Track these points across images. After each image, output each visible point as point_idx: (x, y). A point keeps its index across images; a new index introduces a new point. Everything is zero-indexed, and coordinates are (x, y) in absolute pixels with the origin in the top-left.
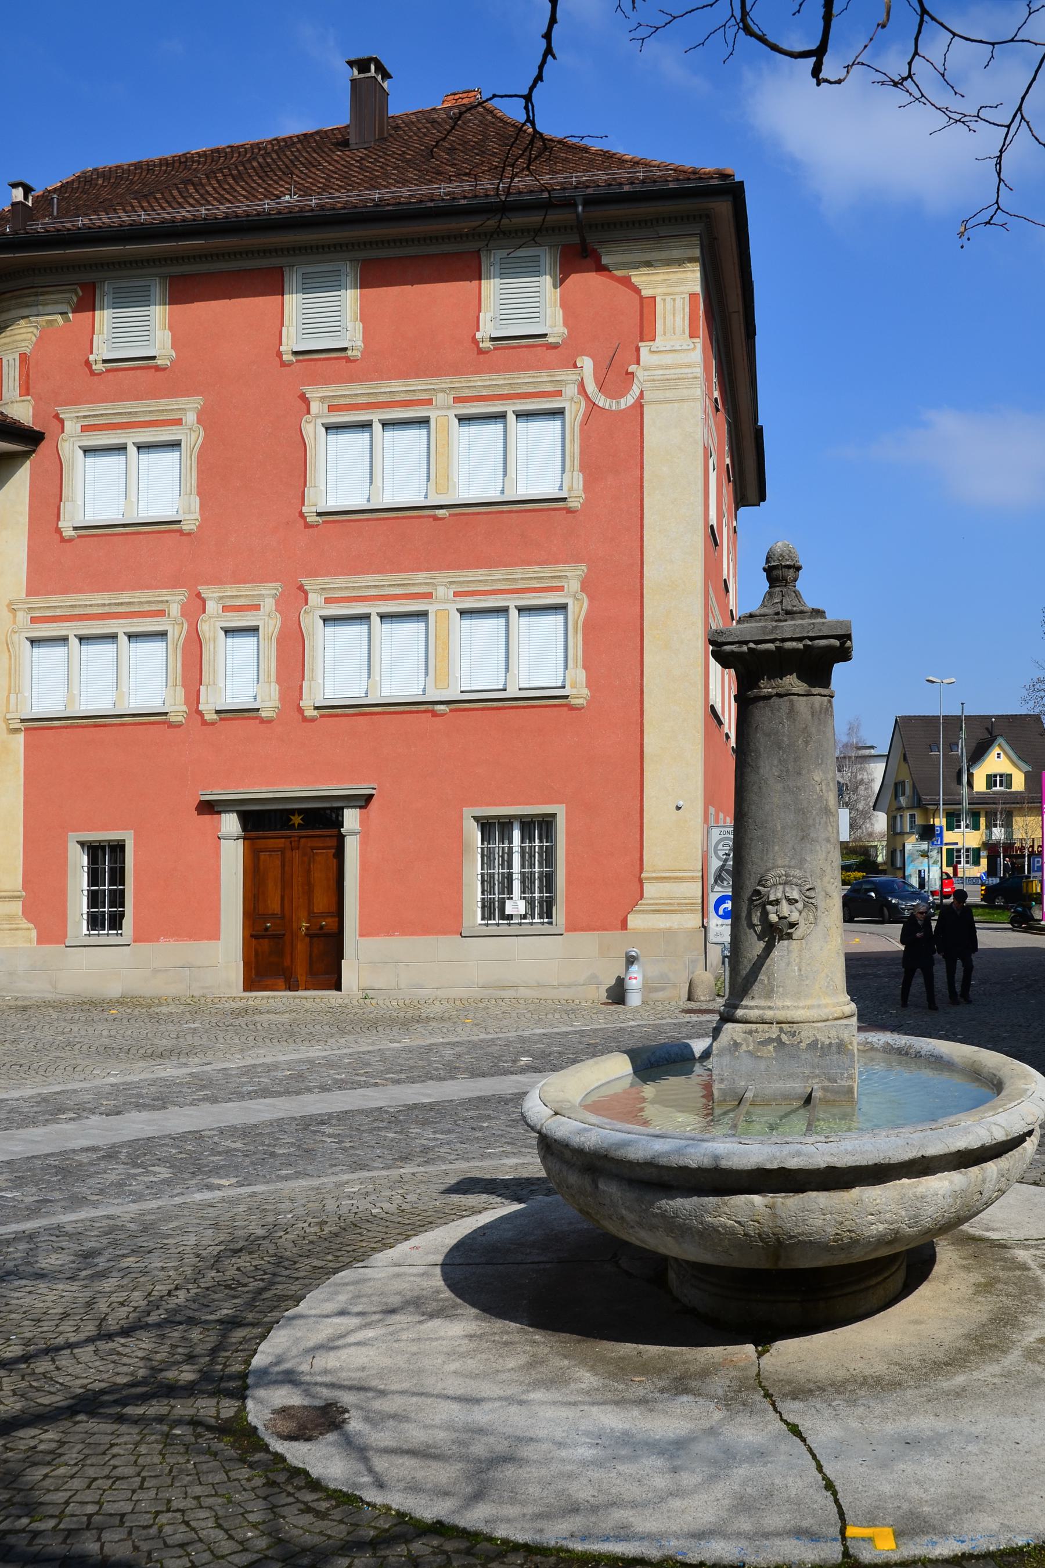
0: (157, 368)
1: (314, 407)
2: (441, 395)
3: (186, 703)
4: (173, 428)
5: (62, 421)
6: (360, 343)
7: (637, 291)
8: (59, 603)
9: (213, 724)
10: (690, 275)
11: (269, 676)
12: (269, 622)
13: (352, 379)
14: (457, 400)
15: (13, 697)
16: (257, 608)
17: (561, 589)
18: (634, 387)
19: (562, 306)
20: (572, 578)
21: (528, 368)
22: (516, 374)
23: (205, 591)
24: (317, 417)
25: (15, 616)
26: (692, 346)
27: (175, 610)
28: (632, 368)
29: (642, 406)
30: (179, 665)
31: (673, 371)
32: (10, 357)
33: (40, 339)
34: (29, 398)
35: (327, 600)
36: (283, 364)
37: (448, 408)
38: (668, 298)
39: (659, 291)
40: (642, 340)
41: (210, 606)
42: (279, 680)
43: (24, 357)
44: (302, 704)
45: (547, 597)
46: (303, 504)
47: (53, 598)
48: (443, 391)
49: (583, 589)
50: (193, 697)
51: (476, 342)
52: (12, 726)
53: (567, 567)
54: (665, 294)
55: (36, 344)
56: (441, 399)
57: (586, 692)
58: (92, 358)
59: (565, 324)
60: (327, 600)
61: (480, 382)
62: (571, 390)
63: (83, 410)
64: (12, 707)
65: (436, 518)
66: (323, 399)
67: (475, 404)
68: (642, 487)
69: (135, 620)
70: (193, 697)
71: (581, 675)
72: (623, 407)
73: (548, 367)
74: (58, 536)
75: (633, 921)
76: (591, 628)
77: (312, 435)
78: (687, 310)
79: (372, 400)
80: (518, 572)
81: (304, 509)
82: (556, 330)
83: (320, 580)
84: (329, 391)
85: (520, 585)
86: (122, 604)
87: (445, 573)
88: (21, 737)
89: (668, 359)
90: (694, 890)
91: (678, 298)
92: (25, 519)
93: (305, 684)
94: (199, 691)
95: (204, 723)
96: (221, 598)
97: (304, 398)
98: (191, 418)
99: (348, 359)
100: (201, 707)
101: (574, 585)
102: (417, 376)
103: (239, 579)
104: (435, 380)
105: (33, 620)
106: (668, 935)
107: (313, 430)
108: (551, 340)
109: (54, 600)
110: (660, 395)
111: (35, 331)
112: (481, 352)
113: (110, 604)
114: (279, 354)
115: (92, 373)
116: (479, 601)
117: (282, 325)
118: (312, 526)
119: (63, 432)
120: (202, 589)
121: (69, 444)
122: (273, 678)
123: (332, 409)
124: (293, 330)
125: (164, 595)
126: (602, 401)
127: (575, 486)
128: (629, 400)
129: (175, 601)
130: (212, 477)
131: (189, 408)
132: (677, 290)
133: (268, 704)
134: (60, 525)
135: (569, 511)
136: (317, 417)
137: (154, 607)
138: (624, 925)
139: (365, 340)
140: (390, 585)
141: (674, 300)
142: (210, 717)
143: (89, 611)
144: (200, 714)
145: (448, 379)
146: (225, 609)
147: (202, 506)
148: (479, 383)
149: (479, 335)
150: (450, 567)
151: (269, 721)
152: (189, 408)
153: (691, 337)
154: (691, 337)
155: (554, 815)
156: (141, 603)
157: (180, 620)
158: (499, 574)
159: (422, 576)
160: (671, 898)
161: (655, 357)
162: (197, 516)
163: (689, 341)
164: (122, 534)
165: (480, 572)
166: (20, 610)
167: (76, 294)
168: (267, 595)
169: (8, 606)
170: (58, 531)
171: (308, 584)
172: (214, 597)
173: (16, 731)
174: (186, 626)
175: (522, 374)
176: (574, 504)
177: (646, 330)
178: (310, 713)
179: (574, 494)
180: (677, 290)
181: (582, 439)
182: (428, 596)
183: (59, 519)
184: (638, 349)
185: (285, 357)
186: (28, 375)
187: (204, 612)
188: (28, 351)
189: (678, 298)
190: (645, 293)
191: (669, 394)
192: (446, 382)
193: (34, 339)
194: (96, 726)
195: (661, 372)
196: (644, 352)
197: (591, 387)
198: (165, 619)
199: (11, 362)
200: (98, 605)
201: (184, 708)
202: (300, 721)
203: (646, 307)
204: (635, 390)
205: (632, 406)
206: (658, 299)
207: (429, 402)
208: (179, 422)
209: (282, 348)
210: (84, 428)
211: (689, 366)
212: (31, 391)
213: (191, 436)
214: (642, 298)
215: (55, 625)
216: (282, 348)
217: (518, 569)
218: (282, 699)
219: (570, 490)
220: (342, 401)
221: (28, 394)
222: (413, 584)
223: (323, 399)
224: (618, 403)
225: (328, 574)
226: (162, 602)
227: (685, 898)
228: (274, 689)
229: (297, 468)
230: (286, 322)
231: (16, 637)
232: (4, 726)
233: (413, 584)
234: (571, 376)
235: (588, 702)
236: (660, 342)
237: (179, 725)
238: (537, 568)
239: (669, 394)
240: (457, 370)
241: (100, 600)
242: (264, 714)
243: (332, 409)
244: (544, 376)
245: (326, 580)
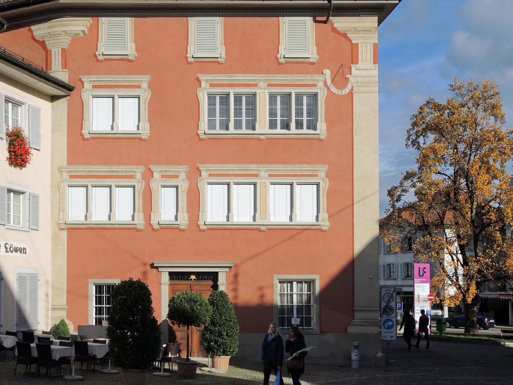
0: (129, 60)
1: (203, 84)
2: (261, 83)
3: (145, 220)
4: (137, 89)
5: (83, 83)
6: (224, 56)
7: (350, 41)
9: (157, 230)
10: (373, 35)
11: (183, 209)
13: (220, 72)
14: (269, 85)
15: (61, 213)
16: (177, 177)
17: (316, 176)
18: (349, 85)
19: (317, 45)
20: (322, 170)
21: (301, 72)
22: (296, 75)
23: (153, 168)
24: (204, 89)
25: (62, 175)
26: (375, 68)
27: (139, 176)
28: (348, 76)
29: (352, 94)
30: (141, 202)
31: (366, 79)
32: (56, 50)
33: (72, 42)
34: (66, 70)
35: (210, 175)
36: (188, 63)
37: (265, 89)
38: (364, 45)
39: (360, 41)
40: (352, 63)
41: (155, 174)
42: (188, 212)
43: (64, 51)
44: (199, 223)
45: (310, 179)
46: (198, 129)
47: (81, 166)
48: (263, 81)
49: (327, 176)
50: (148, 218)
51: (277, 59)
52: (61, 227)
53: (319, 166)
54: (363, 43)
55: (70, 44)
56: (261, 84)
57: (328, 223)
58: (97, 53)
59: (318, 54)
60: (210, 175)
61: (279, 78)
62: (321, 84)
63: (93, 78)
64: (61, 218)
65: (259, 140)
66: (207, 81)
67: (277, 88)
68: (352, 131)
69: (120, 179)
70: (148, 218)
72: (344, 93)
73: (309, 73)
74: (81, 137)
75: (351, 330)
76: (330, 194)
77: (202, 97)
78: (372, 51)
79: (230, 83)
80: (297, 167)
81: (199, 132)
82: (314, 56)
83: (206, 165)
84: (210, 77)
85: (298, 173)
86: (113, 171)
87: (264, 165)
88: (65, 233)
89: (364, 73)
91: (368, 45)
92: (65, 128)
93: (200, 214)
94: (150, 215)
95: (153, 230)
96: (161, 171)
98: (145, 85)
99: (218, 63)
100: (152, 222)
101: (323, 174)
102: (251, 73)
103: (169, 163)
104: (258, 75)
105: (71, 177)
108: (311, 60)
109: (81, 168)
111: (69, 38)
112: (280, 64)
113: (107, 171)
114: (186, 58)
115: (98, 60)
116: (280, 179)
117: (188, 44)
118: (202, 140)
119: (83, 87)
120: (151, 166)
121: (86, 93)
122: (185, 210)
123: (211, 85)
124: (192, 47)
125: (133, 168)
126: (333, 89)
127: (323, 129)
128: (346, 91)
131: (144, 80)
132: (368, 41)
133: (183, 222)
134: (83, 132)
135: (320, 140)
136: (204, 89)
137: (129, 174)
139: (226, 54)
140: (239, 170)
141: (367, 46)
142: (156, 227)
143: (98, 174)
144: (151, 225)
145: (264, 75)
146: (163, 176)
147: (150, 127)
148: (279, 78)
149: (279, 56)
150: (266, 163)
151: (184, 231)
152: (144, 80)
153: (374, 63)
154: (374, 63)
156: (122, 171)
157: (141, 181)
158: (289, 167)
159: (253, 166)
160: (367, 319)
161: (358, 72)
162: (148, 132)
163: (373, 65)
164: (113, 138)
165: (281, 166)
166: (64, 171)
167: (89, 22)
168: (182, 171)
169: (59, 169)
170: (82, 135)
171: (201, 167)
172: (157, 170)
173: (63, 229)
174: (144, 183)
175: (298, 75)
176: (323, 137)
177: (354, 59)
178: (203, 227)
179: (323, 132)
180: (368, 41)
181: (326, 107)
182: (257, 175)
183: (82, 129)
184: (350, 68)
185: (189, 60)
186: (66, 59)
187: (153, 177)
188: (66, 48)
189: (368, 45)
190: (354, 42)
191: (364, 89)
192: (263, 77)
193: (69, 42)
194: (102, 229)
195: (361, 79)
196: (353, 69)
197: (329, 82)
198: (134, 180)
199: (57, 52)
200: (102, 171)
201: (144, 222)
202: (197, 232)
203: (354, 48)
204: (349, 86)
205: (348, 94)
206: (359, 45)
207: (256, 85)
208: (139, 87)
209: (188, 55)
210: (94, 87)
211: (373, 77)
212: (67, 67)
213: (146, 94)
214: (352, 44)
215: (81, 179)
216: (188, 55)
217: (297, 166)
218: (190, 220)
219: (321, 130)
220: (216, 82)
221: (66, 68)
222: (250, 170)
223: (207, 81)
224: (342, 92)
225: (210, 163)
226: (132, 171)
227: (373, 320)
230: (189, 43)
231: (62, 184)
232: (57, 226)
233: (250, 170)
234: (320, 78)
235: (329, 228)
236: (360, 65)
237: (141, 231)
238: (306, 166)
239: (364, 89)
240: (268, 71)
242: (181, 227)
244: (308, 77)
245: (210, 165)
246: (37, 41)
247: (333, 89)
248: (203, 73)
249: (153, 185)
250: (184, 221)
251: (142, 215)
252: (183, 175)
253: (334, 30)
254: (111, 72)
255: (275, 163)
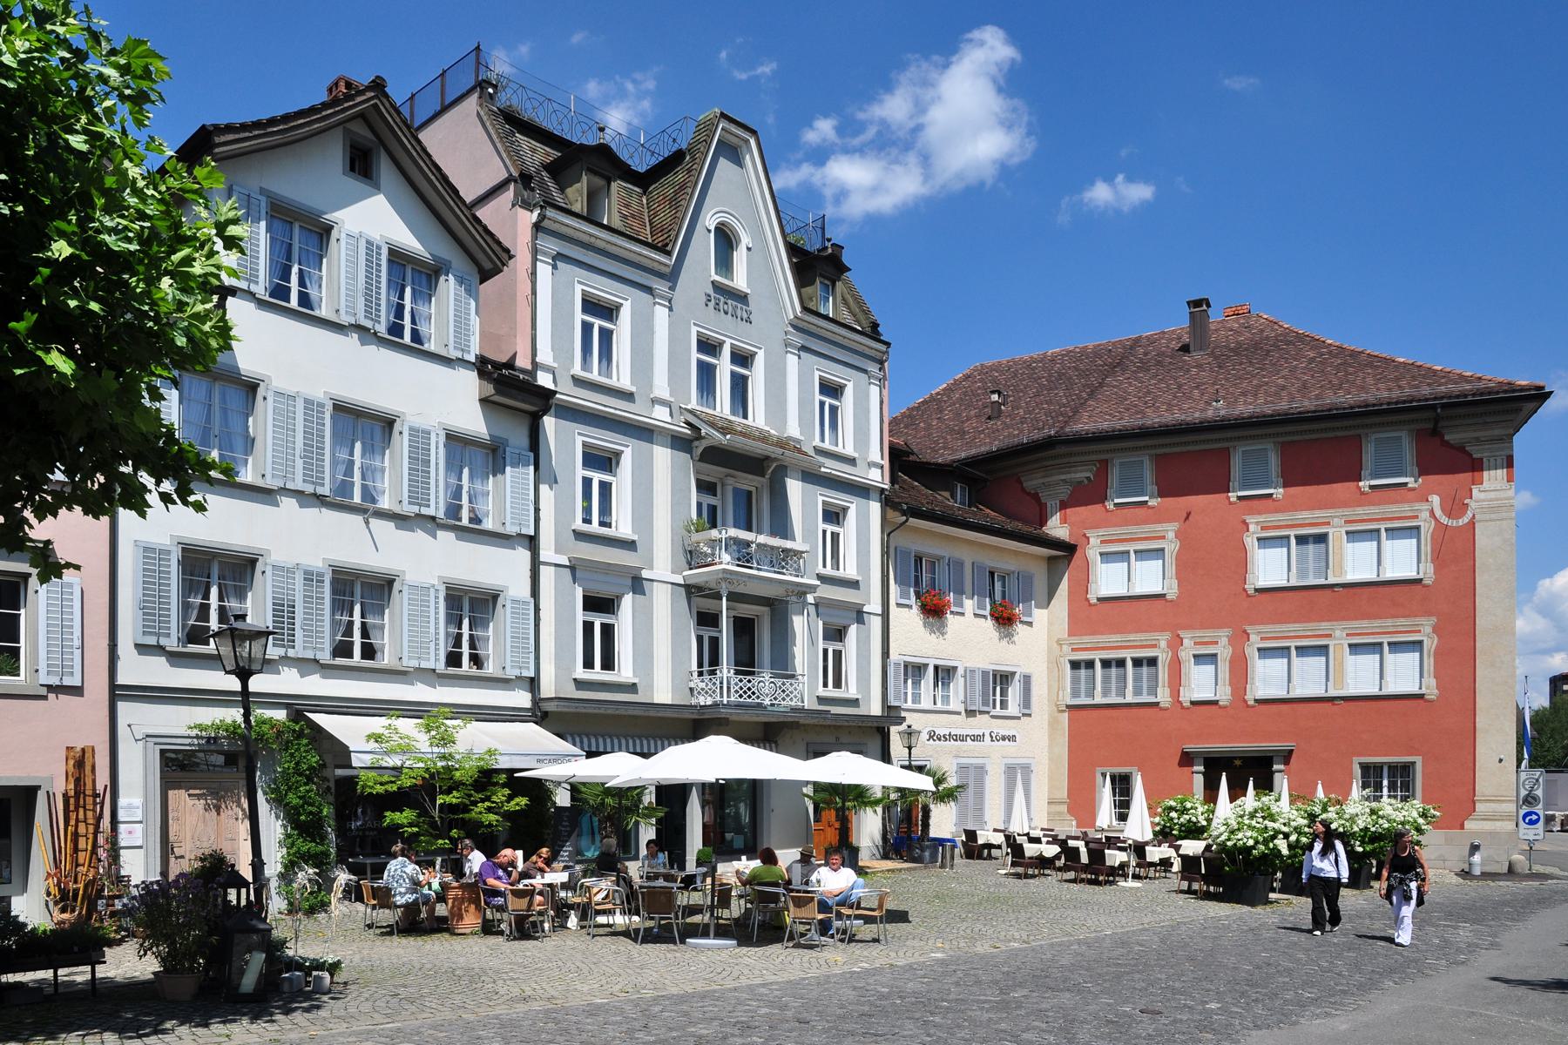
1: (1252, 528)
8: (1088, 640)
12: (1224, 651)
13: (1277, 511)
21: (1396, 502)
27: (1163, 644)
41: (1186, 642)
49: (1436, 630)
71: (1433, 682)
75: (1468, 825)
80: (1389, 622)
84: (1261, 518)
89: (1492, 495)
90: (1512, 807)
97: (1244, 522)
98: (1171, 535)
103: (1203, 626)
106: (1493, 835)
107: (1250, 541)
109: (1086, 639)
110: (1487, 517)
121: (1093, 550)
123: (1263, 528)
125: (1155, 636)
126: (1444, 520)
128: (1466, 520)
129: (1163, 640)
130: (1185, 568)
138: (1462, 827)
150: (1344, 619)
155: (1414, 763)
158: (1377, 623)
159: (1325, 625)
168: (1223, 636)
171: (1249, 629)
176: (1427, 582)
192: (1340, 512)
196: (1475, 492)
204: (1470, 514)
207: (1328, 523)
208: (1163, 537)
213: (1171, 546)
228: (1228, 690)
229: (1242, 564)
234: (1425, 506)
241: (1115, 638)
243: (1263, 528)
244: (1406, 507)
246: (1029, 494)
247: (1444, 520)
248: (1252, 512)
249: (1183, 654)
250: (1224, 695)
251: (1167, 691)
252: (1224, 641)
253: (1447, 444)
254: (1126, 523)
255: (1356, 619)
